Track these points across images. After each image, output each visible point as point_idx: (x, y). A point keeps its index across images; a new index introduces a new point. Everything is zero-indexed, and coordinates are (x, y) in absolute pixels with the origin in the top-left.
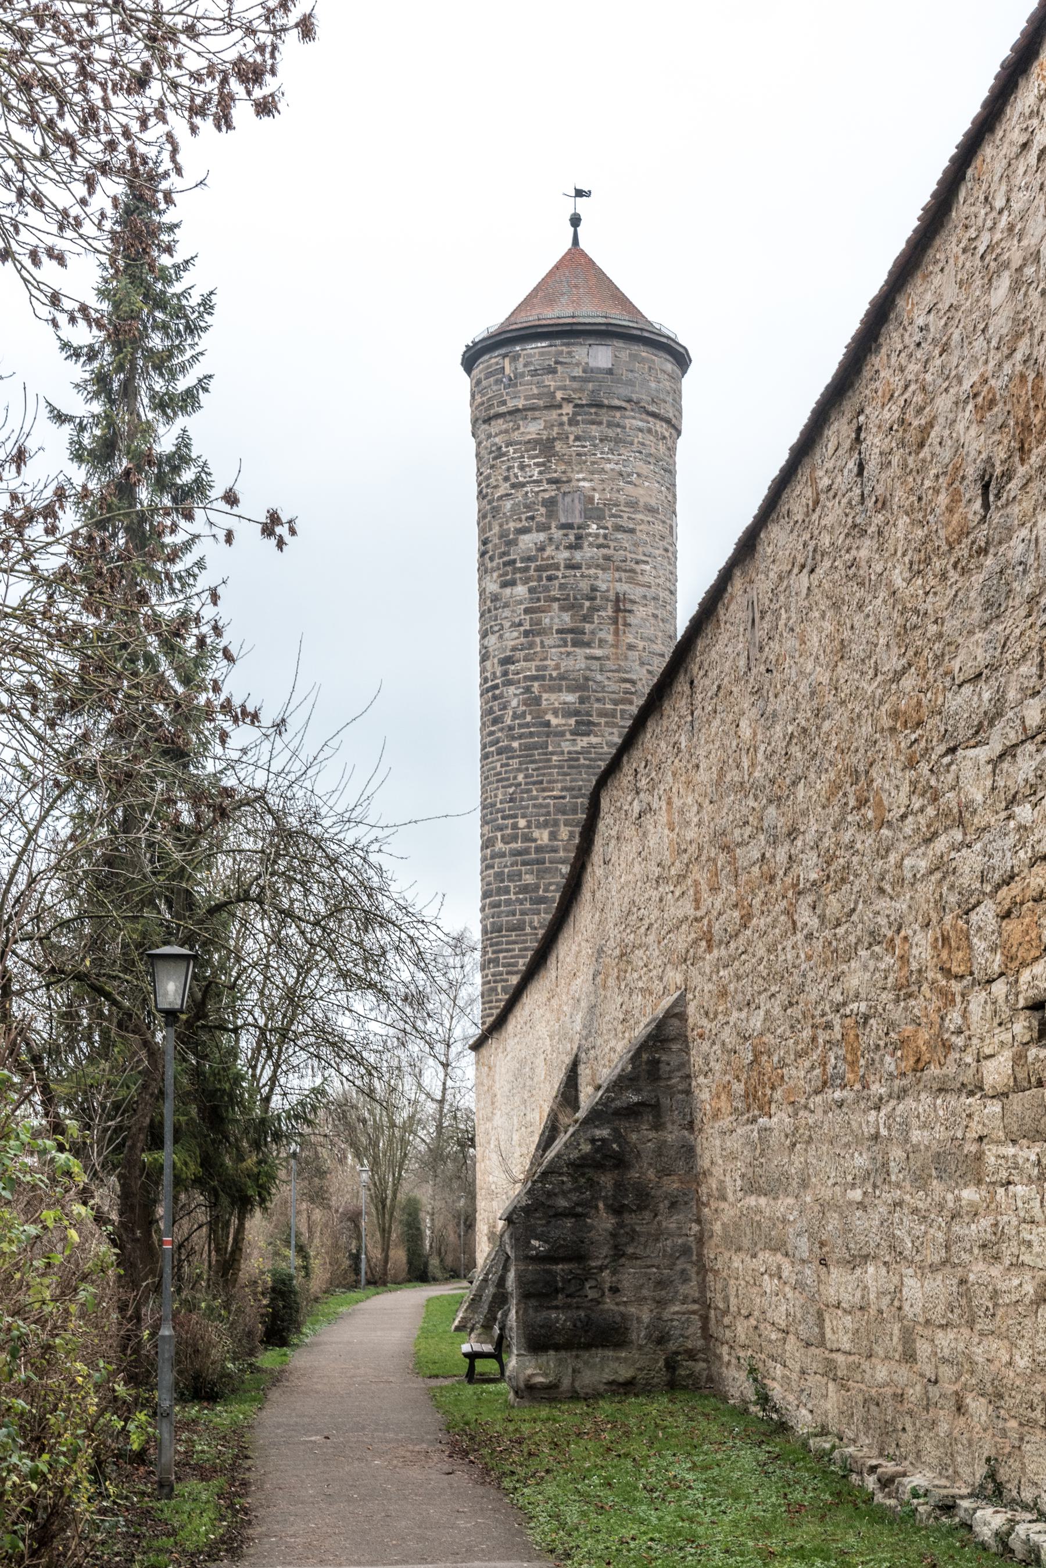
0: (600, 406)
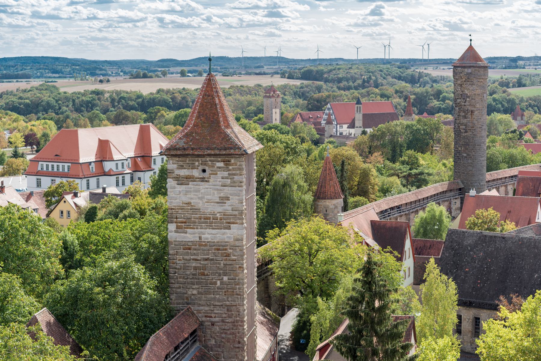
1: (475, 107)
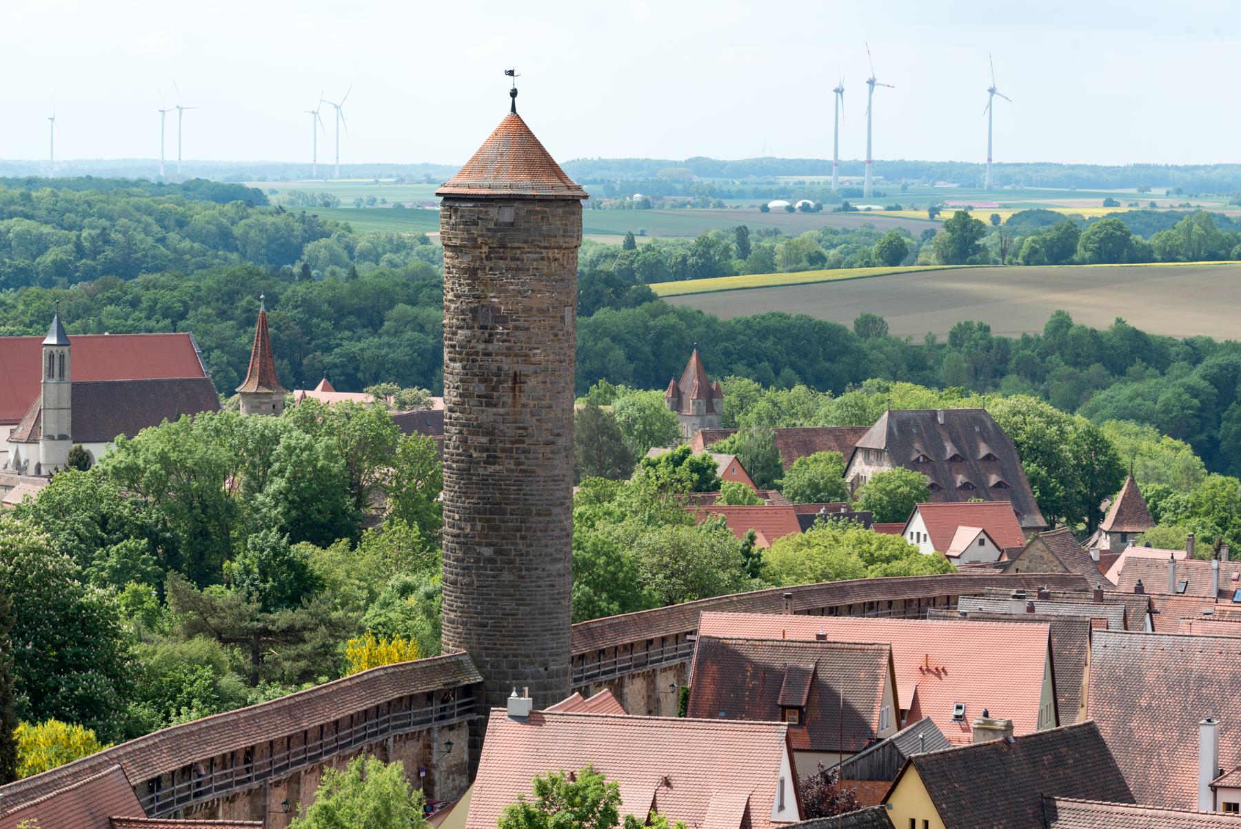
0: (505, 247)
1: (526, 359)
